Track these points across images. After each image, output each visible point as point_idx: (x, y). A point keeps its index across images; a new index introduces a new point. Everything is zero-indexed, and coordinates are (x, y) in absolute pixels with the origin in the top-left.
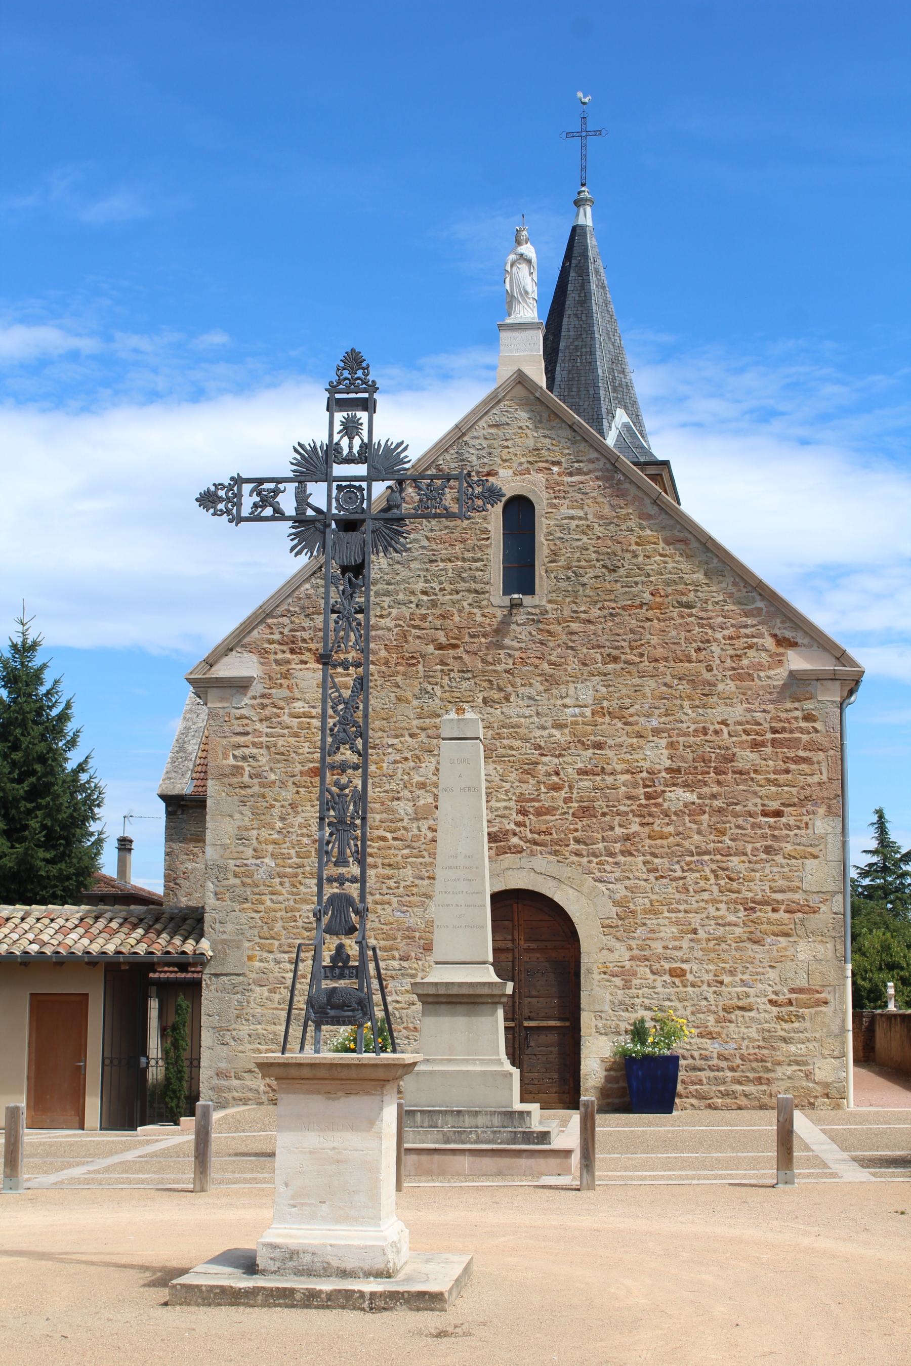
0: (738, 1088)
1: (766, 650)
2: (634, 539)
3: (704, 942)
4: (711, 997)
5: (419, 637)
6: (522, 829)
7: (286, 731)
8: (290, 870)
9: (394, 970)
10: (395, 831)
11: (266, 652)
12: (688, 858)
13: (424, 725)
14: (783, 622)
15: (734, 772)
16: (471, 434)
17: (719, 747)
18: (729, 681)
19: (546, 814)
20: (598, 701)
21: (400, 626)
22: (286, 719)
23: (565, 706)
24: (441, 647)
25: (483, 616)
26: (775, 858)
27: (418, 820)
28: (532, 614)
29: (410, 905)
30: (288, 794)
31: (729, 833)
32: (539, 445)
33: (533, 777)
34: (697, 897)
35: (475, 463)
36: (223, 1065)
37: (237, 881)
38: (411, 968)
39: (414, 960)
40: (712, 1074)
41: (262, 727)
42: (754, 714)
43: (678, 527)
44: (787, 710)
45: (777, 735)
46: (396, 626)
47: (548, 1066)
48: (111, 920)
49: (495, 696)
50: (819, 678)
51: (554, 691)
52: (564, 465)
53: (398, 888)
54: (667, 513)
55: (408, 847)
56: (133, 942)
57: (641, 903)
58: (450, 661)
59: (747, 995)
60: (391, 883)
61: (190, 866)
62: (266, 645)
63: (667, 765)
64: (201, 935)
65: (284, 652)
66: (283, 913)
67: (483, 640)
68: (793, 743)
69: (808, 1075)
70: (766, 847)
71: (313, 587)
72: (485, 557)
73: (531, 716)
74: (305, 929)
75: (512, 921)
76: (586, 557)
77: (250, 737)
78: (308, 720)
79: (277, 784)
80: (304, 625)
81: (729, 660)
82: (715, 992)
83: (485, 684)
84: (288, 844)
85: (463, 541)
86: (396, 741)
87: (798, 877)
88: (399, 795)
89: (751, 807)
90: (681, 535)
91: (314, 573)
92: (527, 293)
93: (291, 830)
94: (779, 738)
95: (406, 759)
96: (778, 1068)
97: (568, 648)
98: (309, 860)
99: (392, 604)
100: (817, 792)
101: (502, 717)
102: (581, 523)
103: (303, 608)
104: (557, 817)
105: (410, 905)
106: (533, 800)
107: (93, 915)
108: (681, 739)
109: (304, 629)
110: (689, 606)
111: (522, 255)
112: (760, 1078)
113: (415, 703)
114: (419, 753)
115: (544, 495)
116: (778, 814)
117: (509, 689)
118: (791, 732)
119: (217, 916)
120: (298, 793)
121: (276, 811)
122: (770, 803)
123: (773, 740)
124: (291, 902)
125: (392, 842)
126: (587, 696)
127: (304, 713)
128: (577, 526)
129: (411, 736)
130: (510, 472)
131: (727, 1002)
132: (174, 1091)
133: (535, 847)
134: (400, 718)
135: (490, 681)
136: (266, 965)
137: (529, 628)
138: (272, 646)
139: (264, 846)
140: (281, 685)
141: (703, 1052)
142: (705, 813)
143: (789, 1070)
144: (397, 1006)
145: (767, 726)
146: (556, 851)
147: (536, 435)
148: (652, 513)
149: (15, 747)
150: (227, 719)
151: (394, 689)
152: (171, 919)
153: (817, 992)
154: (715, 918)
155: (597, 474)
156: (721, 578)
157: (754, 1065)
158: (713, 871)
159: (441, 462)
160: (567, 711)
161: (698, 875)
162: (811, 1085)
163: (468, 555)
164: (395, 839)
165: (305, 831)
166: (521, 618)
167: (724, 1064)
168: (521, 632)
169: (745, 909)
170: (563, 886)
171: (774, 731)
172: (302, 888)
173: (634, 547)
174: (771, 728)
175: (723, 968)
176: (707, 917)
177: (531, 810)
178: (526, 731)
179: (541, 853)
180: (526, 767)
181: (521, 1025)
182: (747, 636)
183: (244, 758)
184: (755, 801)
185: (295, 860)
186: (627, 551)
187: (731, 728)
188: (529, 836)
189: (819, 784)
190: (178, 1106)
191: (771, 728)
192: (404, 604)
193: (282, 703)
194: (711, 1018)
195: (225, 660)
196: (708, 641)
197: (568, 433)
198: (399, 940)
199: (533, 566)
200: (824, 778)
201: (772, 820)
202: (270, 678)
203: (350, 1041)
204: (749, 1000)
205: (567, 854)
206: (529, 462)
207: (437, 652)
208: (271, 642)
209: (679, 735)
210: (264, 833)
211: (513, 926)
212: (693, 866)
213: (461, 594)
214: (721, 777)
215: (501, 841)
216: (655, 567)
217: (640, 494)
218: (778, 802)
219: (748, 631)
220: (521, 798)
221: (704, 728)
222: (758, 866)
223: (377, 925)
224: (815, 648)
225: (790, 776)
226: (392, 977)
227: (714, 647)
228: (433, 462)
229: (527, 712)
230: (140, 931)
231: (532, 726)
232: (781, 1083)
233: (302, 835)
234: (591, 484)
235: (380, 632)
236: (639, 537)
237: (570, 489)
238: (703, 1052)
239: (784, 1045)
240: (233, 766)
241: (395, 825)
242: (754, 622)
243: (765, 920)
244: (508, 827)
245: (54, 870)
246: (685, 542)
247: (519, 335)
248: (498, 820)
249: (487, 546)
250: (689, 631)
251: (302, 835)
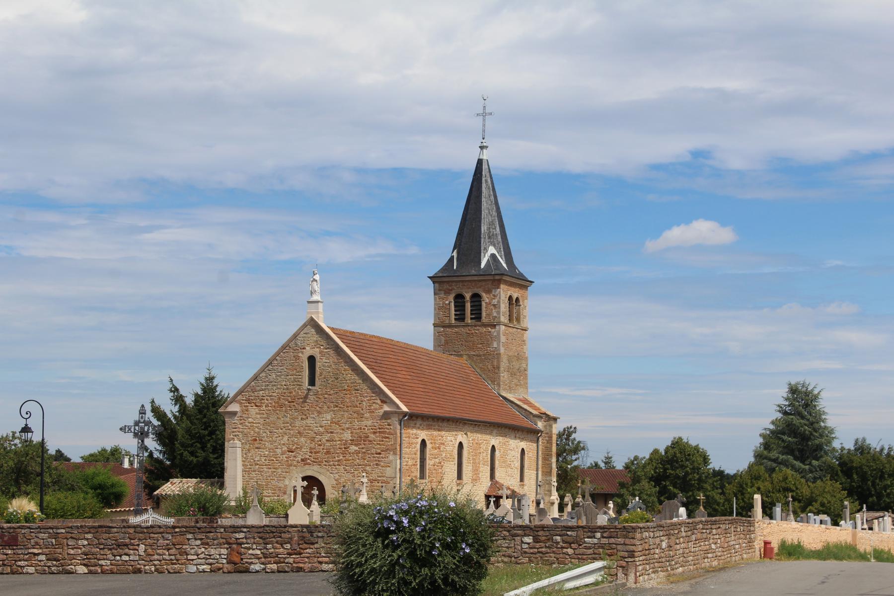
20: (332, 419)
57: (342, 480)
68: (384, 432)
126: (329, 417)
149: (205, 417)
220: (311, 448)
234: (332, 352)
245: (216, 461)
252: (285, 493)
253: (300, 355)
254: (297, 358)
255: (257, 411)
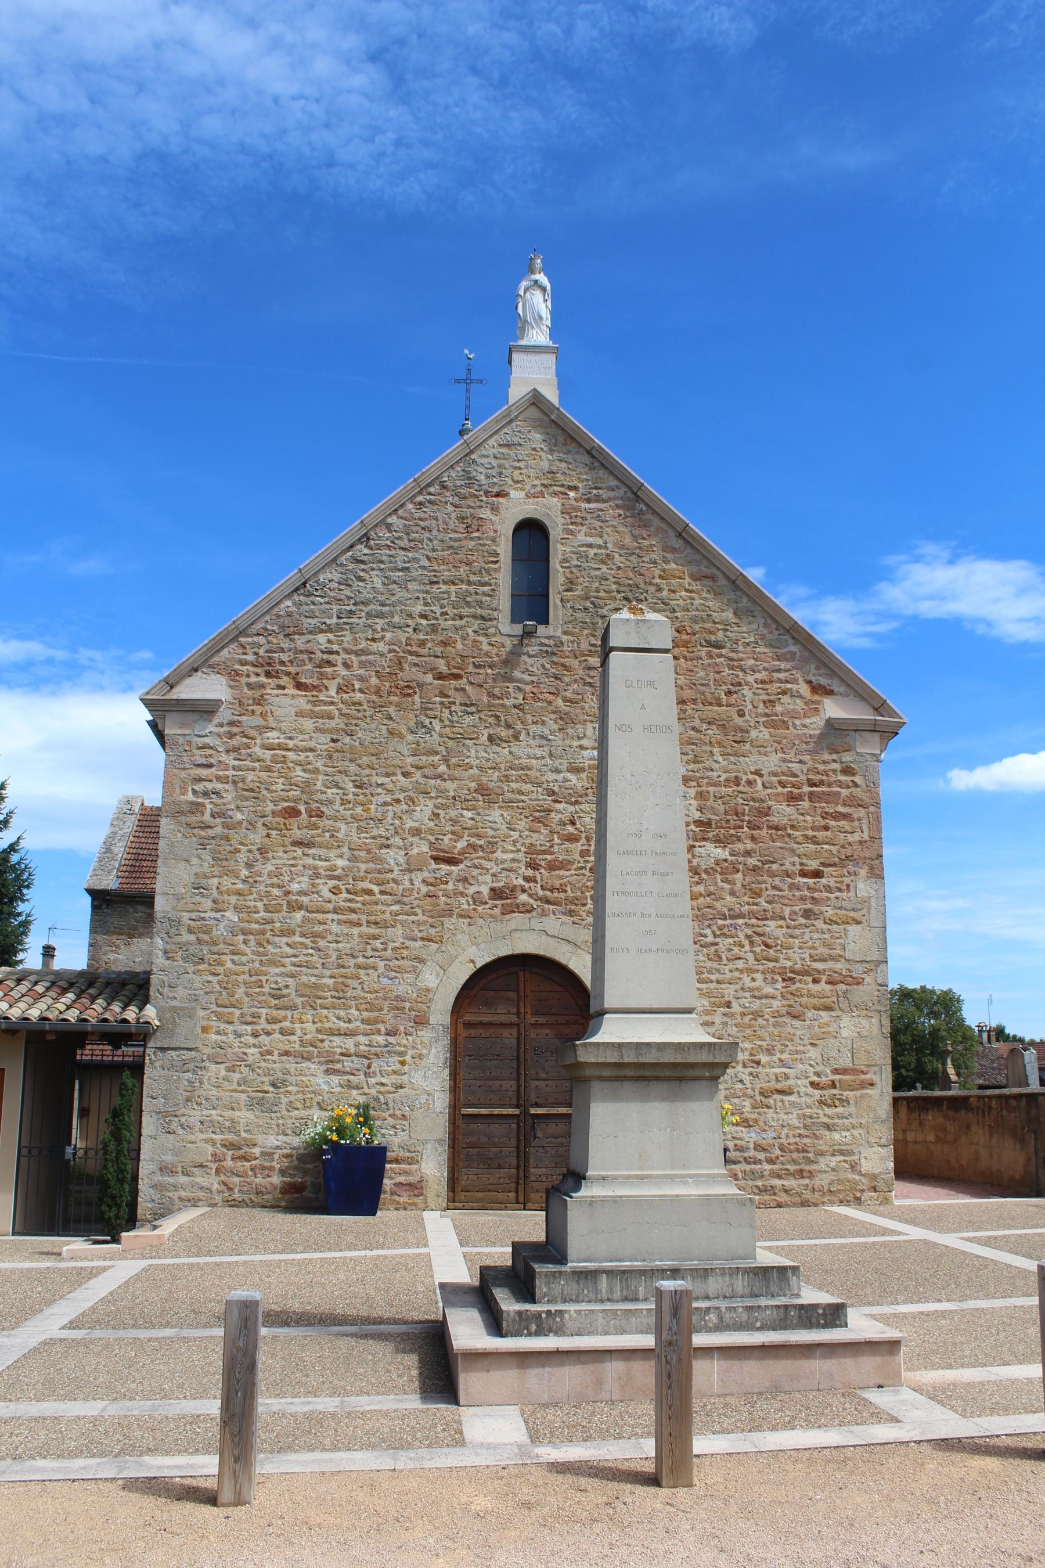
0: (777, 1182)
1: (801, 697)
2: (657, 572)
3: (739, 1017)
4: (747, 1079)
5: (416, 665)
6: (532, 884)
7: (257, 764)
8: (256, 926)
9: (379, 1046)
10: (383, 884)
11: (238, 674)
12: (720, 922)
13: (420, 763)
14: (818, 668)
15: (769, 827)
16: (479, 452)
17: (753, 800)
18: (762, 728)
19: (559, 869)
21: (395, 651)
22: (257, 750)
23: (582, 748)
24: (440, 677)
25: (490, 644)
26: (816, 923)
27: (410, 871)
28: (546, 645)
29: (399, 970)
30: (257, 837)
31: (765, 894)
32: (554, 468)
33: (545, 825)
34: (731, 966)
35: (483, 482)
36: (168, 1158)
37: (192, 938)
38: (399, 1044)
39: (403, 1035)
40: (748, 1168)
41: (229, 760)
42: (790, 765)
43: (705, 562)
44: (824, 762)
45: (814, 789)
46: (390, 651)
47: (558, 1160)
48: (36, 983)
49: (503, 734)
50: (857, 728)
51: (570, 731)
52: (581, 491)
53: (385, 950)
54: (693, 547)
55: (398, 902)
56: (62, 1007)
58: (451, 692)
59: (787, 1077)
60: (377, 944)
61: (112, 956)
62: (237, 667)
63: (696, 817)
64: (145, 1001)
65: (258, 675)
66: (246, 977)
67: (489, 671)
69: (853, 1167)
70: (805, 910)
71: (295, 604)
72: (493, 581)
73: (543, 758)
74: (273, 996)
75: (518, 991)
76: (606, 588)
77: (213, 770)
78: (284, 753)
79: (244, 825)
80: (282, 645)
81: (761, 706)
82: (751, 1074)
83: (491, 720)
84: (255, 896)
85: (469, 564)
86: (386, 780)
87: (840, 944)
88: (389, 842)
89: (788, 867)
90: (708, 571)
91: (297, 590)
92: (541, 318)
93: (258, 879)
94: (813, 792)
95: (398, 801)
96: (821, 1159)
97: (585, 684)
98: (280, 915)
99: (386, 626)
100: (858, 852)
101: (510, 758)
102: (600, 551)
103: (283, 627)
104: (573, 872)
105: (399, 970)
106: (545, 852)
107: (15, 977)
108: (711, 789)
109: (282, 650)
110: (718, 646)
111: (536, 282)
112: (801, 1171)
113: (410, 737)
114: (413, 795)
115: (560, 520)
116: (817, 874)
117: (519, 727)
118: (830, 785)
119: (166, 979)
120: (268, 836)
121: (242, 857)
122: (809, 862)
123: (811, 794)
124: (257, 965)
125: (378, 896)
127: (279, 745)
128: (595, 554)
129: (404, 775)
130: (522, 494)
131: (764, 1085)
132: (113, 1197)
133: (546, 906)
134: (391, 754)
135: (497, 717)
136: (224, 1038)
137: (542, 661)
138: (244, 668)
139: (226, 897)
140: (253, 711)
141: (738, 1142)
142: (738, 871)
143: (833, 1161)
144: (382, 1089)
145: (804, 778)
146: (570, 911)
147: (550, 457)
148: (677, 546)
150: (187, 748)
151: (386, 722)
152: (108, 984)
153: (863, 1072)
154: (751, 990)
155: (617, 502)
156: (751, 618)
157: (795, 1155)
158: (748, 937)
159: (445, 479)
160: (585, 753)
161: (731, 940)
162: (857, 1177)
163: (474, 578)
164: (382, 893)
165: (275, 880)
166: (533, 649)
167: (761, 1156)
168: (533, 665)
169: (784, 980)
170: (580, 951)
171: (812, 784)
172: (270, 947)
173: (658, 581)
174: (808, 780)
175: (760, 1046)
176: (742, 989)
177: (543, 863)
178: (538, 774)
179: (554, 913)
180: (537, 814)
181: (526, 1112)
182: (780, 681)
183: (206, 794)
184: (792, 859)
185: (262, 914)
186: (650, 583)
187: (766, 778)
188: (541, 893)
189: (860, 842)
190: (117, 1217)
191: (808, 780)
192: (400, 628)
193: (253, 733)
194: (747, 1103)
195: (188, 681)
196: (739, 684)
197: (587, 459)
198: (385, 1012)
199: (546, 595)
200: (866, 836)
201: (811, 881)
202: (241, 703)
203: (331, 1131)
204: (788, 1083)
205: (584, 914)
206: (543, 485)
207: (436, 682)
208: (243, 663)
209: (709, 784)
210: (227, 882)
211: (519, 997)
212: (725, 931)
213: (465, 619)
214: (756, 833)
215: (507, 898)
216: (681, 602)
217: (664, 526)
218: (817, 862)
219: (782, 676)
220: (531, 850)
221: (736, 777)
222: (797, 932)
223: (359, 992)
224: (852, 697)
225: (829, 833)
226: (377, 1055)
227: (746, 691)
228: (436, 478)
229: (539, 752)
230: (71, 996)
231: (545, 769)
232: (824, 1176)
233: (272, 885)
234: (611, 513)
235: (371, 657)
236: (664, 570)
237: (588, 516)
238: (738, 1142)
239: (827, 1133)
240: (192, 803)
241: (383, 876)
242: (788, 667)
243: (805, 992)
244: (515, 883)
246: (713, 578)
247: (533, 358)
248: (505, 873)
249: (495, 570)
250: (718, 673)
251: (272, 885)
252: (421, 1021)
253: (486, 514)
254: (471, 525)
255: (302, 702)
